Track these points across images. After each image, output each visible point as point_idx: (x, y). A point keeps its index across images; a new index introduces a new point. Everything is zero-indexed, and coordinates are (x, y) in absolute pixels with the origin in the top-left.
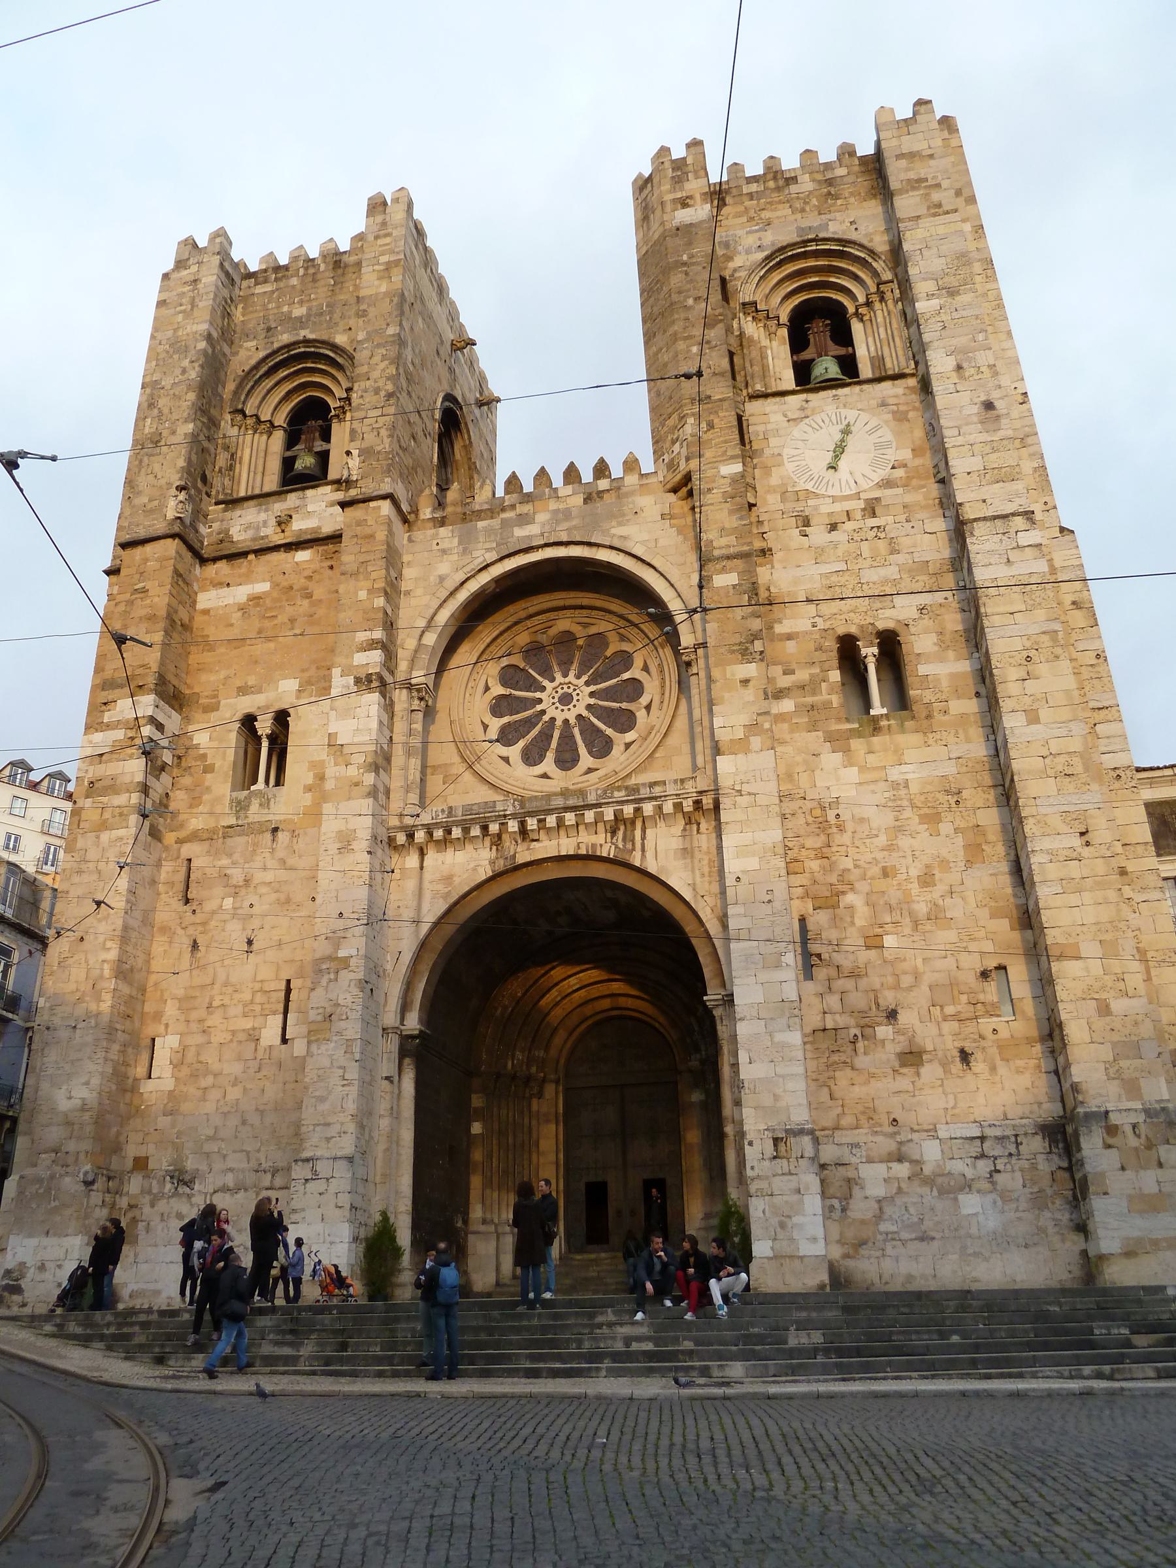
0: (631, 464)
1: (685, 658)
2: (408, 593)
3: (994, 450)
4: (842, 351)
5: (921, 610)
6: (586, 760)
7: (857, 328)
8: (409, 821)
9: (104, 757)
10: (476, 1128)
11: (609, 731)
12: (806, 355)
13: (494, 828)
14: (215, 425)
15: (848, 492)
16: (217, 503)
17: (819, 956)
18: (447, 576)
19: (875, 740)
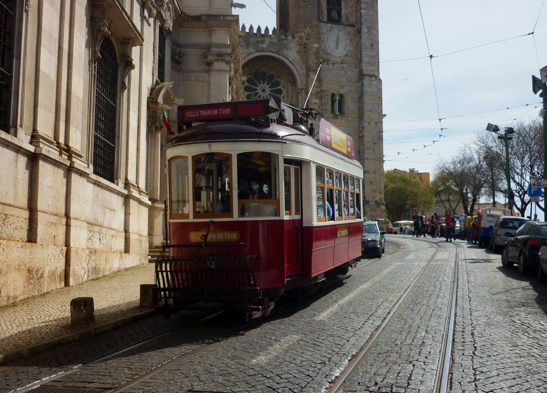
1: (299, 91)
3: (371, 57)
5: (349, 91)
15: (338, 56)
19: (337, 120)
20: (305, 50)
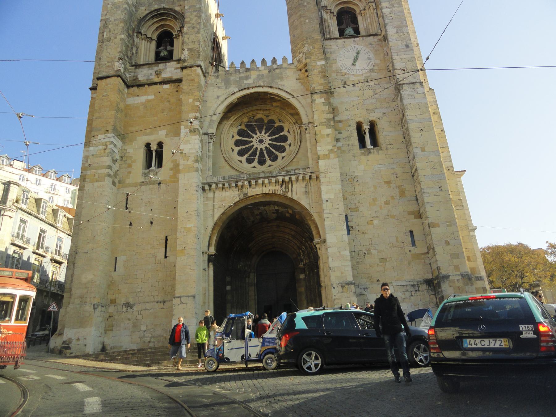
0: (285, 59)
2: (206, 101)
3: (409, 61)
4: (355, 26)
6: (269, 162)
7: (360, 19)
8: (209, 180)
9: (94, 156)
10: (228, 288)
11: (276, 153)
12: (342, 27)
13: (240, 184)
14: (130, 37)
15: (359, 74)
16: (132, 66)
17: (352, 227)
18: (220, 96)
19: (370, 157)
20: (306, 74)
